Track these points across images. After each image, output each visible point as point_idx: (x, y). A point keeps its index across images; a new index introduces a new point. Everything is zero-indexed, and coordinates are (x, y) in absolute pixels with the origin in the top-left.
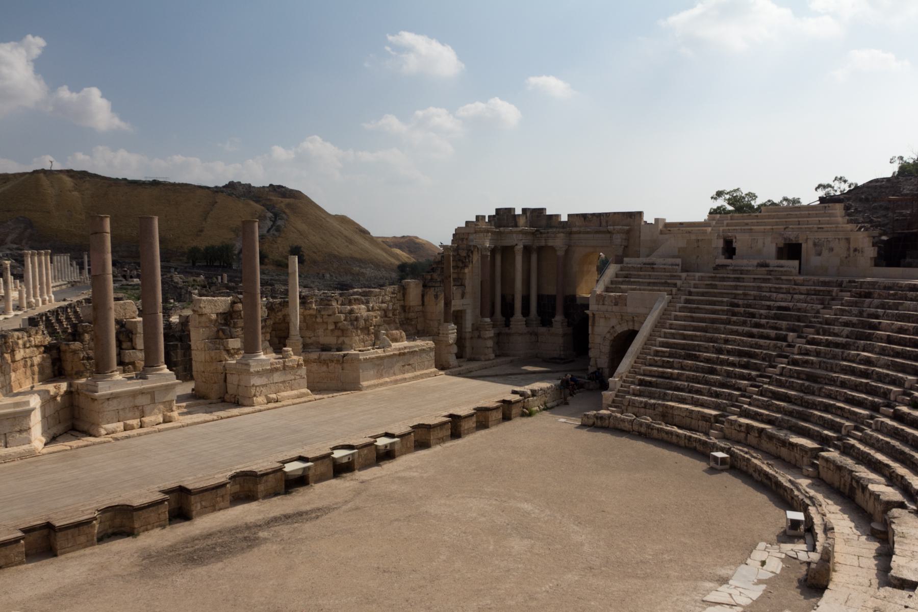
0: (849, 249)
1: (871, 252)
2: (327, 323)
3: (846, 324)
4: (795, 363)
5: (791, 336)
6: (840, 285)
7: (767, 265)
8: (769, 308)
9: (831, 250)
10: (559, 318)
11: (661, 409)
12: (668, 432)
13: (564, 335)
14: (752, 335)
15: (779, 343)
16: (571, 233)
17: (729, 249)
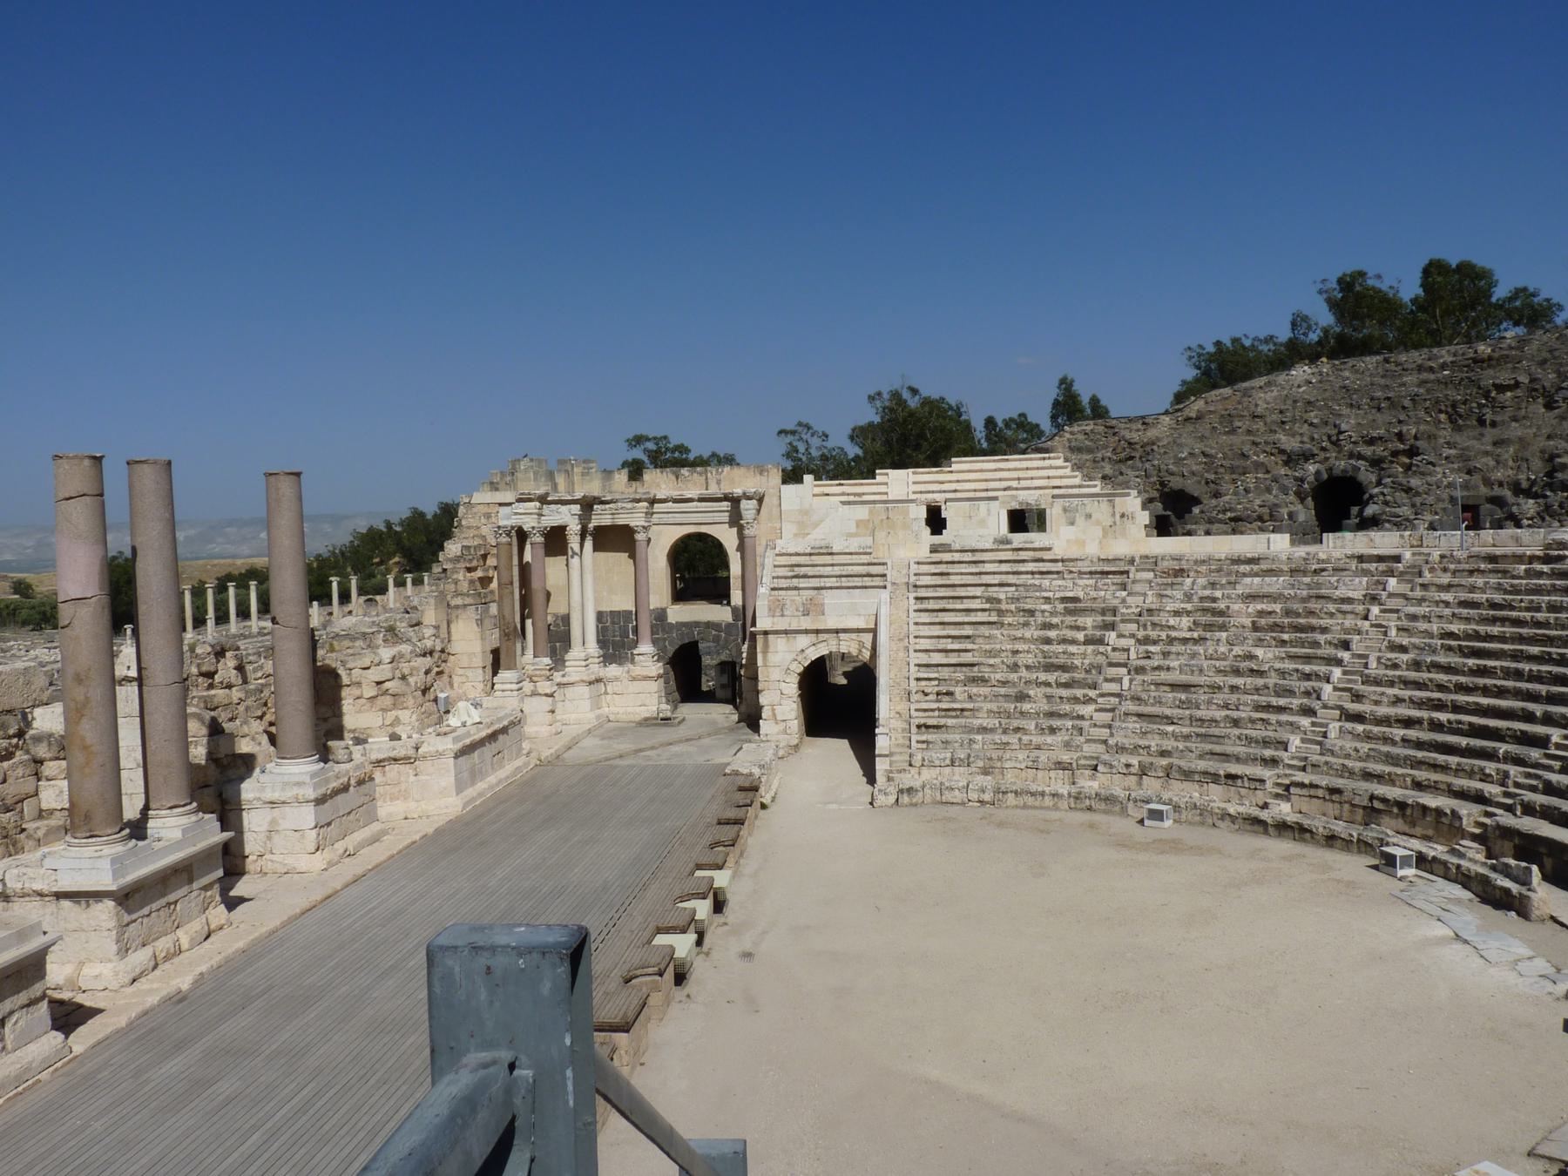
0: (1114, 514)
1: (1144, 518)
2: (359, 684)
3: (1177, 613)
4: (1140, 670)
5: (1111, 637)
6: (1132, 561)
7: (1008, 542)
8: (1047, 600)
9: (1089, 516)
10: (646, 647)
11: (981, 764)
12: (1033, 794)
13: (659, 676)
14: (1048, 641)
15: (1102, 649)
16: (653, 502)
17: (936, 521)
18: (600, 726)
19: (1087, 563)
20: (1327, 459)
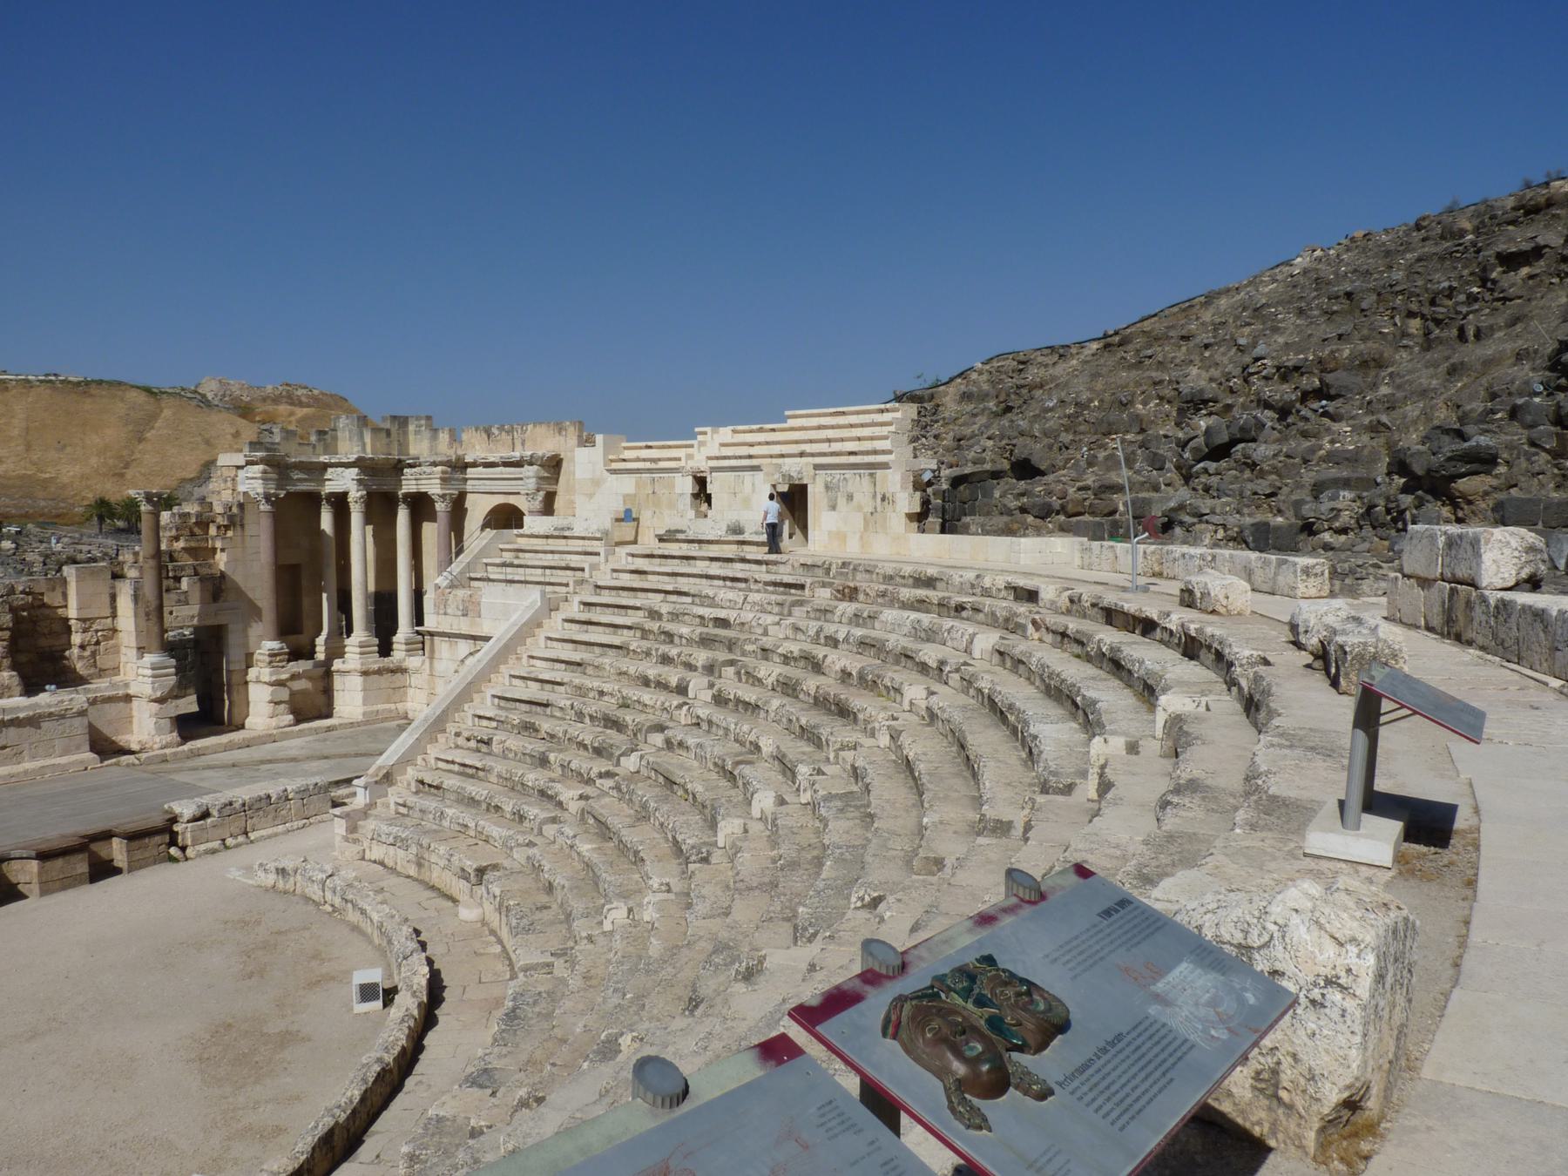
0: (874, 496)
18: (366, 723)
19: (788, 569)
20: (1229, 408)
